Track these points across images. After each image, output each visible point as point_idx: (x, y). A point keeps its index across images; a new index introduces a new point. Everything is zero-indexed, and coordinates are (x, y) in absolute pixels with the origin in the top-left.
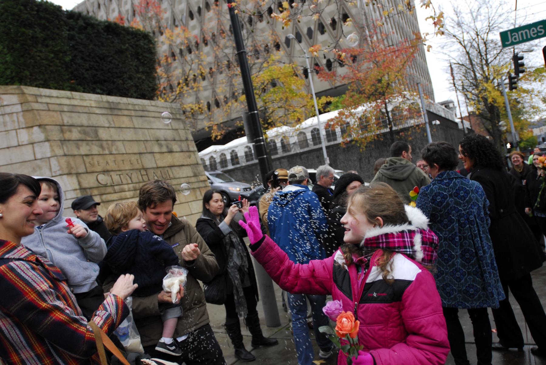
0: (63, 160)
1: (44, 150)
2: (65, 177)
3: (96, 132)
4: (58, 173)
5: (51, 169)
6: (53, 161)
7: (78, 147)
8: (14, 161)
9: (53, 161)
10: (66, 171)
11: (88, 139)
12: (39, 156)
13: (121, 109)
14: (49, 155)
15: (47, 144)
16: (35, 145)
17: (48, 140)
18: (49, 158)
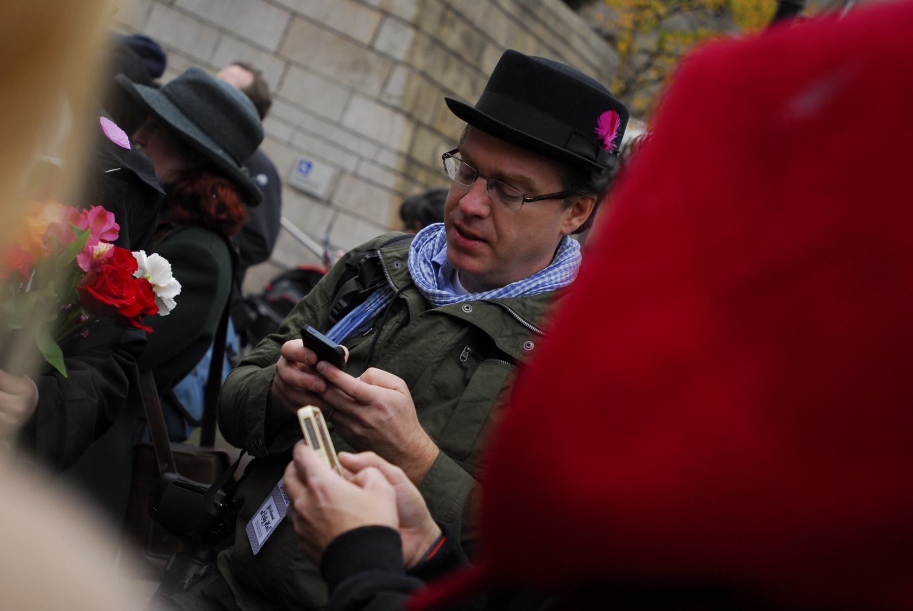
0: (417, 81)
1: (398, 41)
2: (400, 119)
3: (482, 49)
4: (394, 102)
5: (385, 84)
6: (399, 76)
7: (446, 66)
8: (331, 23)
9: (399, 76)
10: (407, 108)
11: (467, 57)
12: (381, 45)
13: (535, 18)
14: (400, 55)
15: (410, 33)
16: (389, 21)
17: (416, 26)
18: (396, 63)
